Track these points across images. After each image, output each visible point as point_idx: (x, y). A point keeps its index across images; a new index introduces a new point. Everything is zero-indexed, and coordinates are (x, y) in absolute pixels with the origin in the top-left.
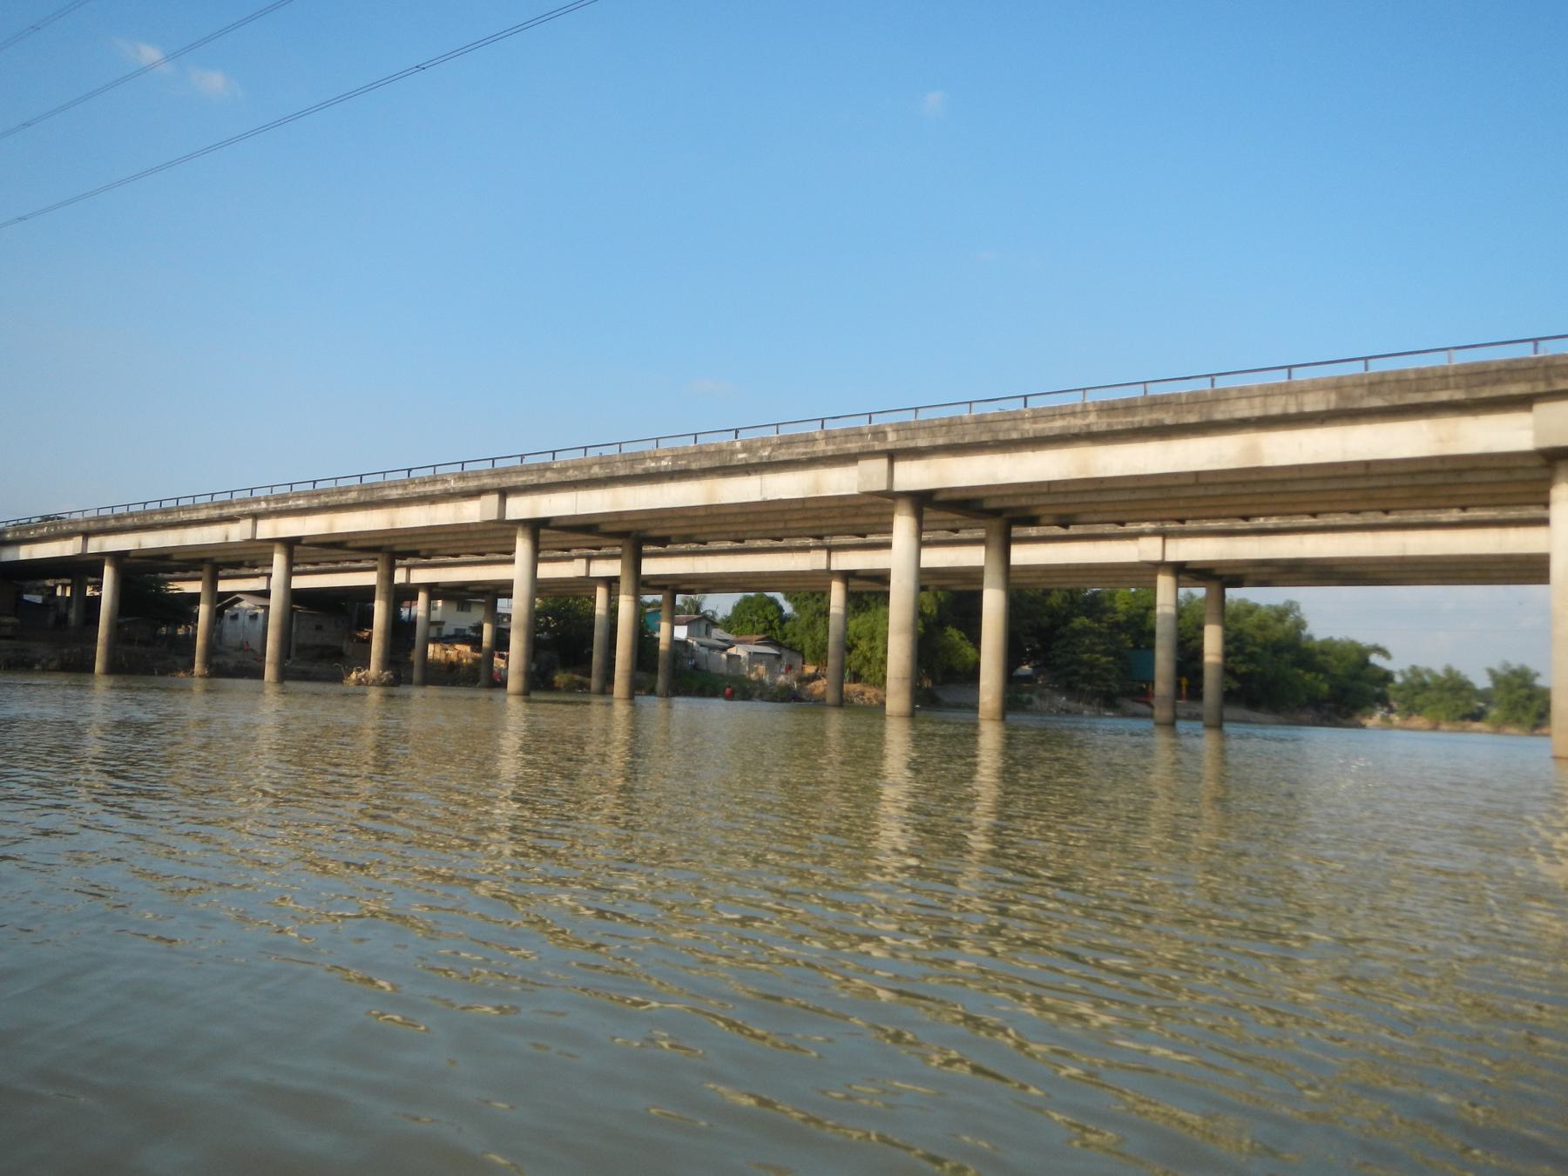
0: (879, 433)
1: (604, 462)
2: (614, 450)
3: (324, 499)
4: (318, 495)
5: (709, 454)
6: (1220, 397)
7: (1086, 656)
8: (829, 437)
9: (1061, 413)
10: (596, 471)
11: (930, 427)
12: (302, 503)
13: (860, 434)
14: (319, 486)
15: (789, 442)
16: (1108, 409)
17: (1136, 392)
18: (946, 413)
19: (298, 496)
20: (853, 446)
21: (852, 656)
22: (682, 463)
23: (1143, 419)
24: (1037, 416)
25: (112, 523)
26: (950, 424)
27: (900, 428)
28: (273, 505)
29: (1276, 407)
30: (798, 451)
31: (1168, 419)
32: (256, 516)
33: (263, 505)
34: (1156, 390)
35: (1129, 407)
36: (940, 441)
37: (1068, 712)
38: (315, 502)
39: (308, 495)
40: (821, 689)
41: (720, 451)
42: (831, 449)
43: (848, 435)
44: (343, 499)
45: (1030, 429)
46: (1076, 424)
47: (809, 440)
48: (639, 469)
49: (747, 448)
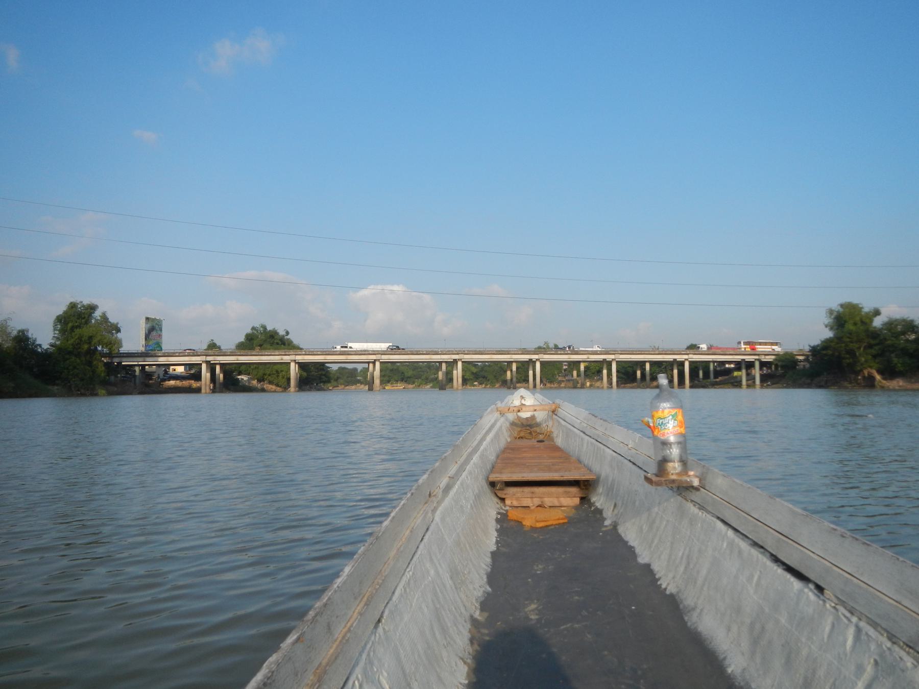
0: (464, 351)
1: (410, 351)
2: (412, 349)
3: (327, 353)
4: (326, 352)
5: (434, 352)
6: (510, 351)
7: (313, 373)
8: (456, 351)
9: (490, 351)
10: (409, 353)
11: (472, 351)
12: (319, 353)
13: (461, 351)
14: (324, 350)
15: (449, 351)
16: (496, 351)
17: (499, 349)
18: (474, 349)
19: (318, 352)
20: (460, 353)
21: (270, 377)
22: (428, 353)
23: (500, 353)
24: (487, 351)
25: (229, 354)
26: (475, 351)
27: (468, 351)
28: (307, 353)
29: (516, 353)
30: (451, 352)
31: (504, 353)
32: (296, 355)
33: (304, 353)
34: (503, 349)
35: (499, 351)
36: (474, 353)
37: (309, 390)
38: (325, 353)
39: (321, 351)
40: (270, 388)
41: (436, 351)
42: (456, 353)
43: (459, 351)
44: (335, 353)
45: (486, 352)
46: (493, 352)
47: (452, 351)
48: (419, 353)
49: (441, 351)
